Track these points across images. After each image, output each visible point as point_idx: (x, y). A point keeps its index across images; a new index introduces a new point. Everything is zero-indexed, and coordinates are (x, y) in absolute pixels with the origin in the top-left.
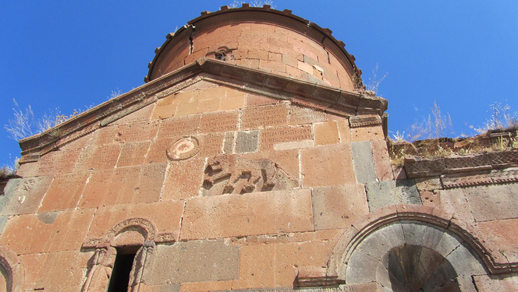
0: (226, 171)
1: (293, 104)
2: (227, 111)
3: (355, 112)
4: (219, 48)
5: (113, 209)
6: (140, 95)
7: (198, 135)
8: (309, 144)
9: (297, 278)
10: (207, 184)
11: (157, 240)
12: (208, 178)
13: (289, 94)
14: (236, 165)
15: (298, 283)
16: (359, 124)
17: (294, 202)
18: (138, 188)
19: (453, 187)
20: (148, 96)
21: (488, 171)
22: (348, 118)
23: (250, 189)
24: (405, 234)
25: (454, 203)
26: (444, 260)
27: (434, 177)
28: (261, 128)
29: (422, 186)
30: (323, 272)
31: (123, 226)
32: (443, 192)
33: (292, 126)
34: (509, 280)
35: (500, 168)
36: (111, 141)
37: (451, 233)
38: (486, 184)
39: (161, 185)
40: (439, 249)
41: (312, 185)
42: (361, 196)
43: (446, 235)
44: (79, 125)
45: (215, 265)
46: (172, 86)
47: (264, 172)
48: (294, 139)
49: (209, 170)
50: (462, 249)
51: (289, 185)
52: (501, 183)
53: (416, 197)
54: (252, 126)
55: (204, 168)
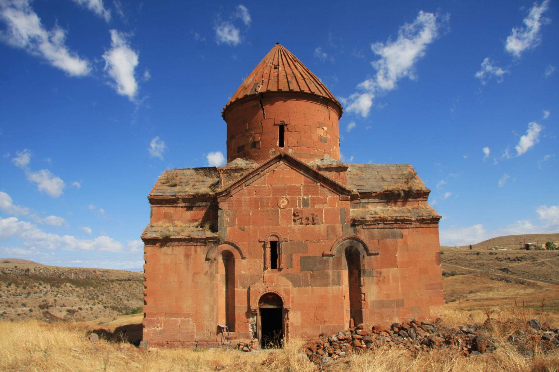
0: (301, 216)
1: (321, 185)
2: (296, 185)
3: (342, 194)
4: (280, 122)
5: (265, 227)
6: (258, 170)
7: (288, 197)
8: (327, 206)
9: (323, 253)
10: (295, 221)
11: (283, 240)
12: (295, 218)
13: (320, 181)
14: (304, 214)
15: (323, 255)
16: (343, 199)
17: (322, 229)
18: (271, 219)
19: (365, 229)
20: (262, 171)
21: (375, 224)
22: (340, 196)
23: (309, 224)
24: (351, 243)
25: (364, 234)
26: (358, 250)
27: (361, 225)
28: (310, 196)
29: (357, 227)
30: (330, 253)
31: (271, 235)
32: (363, 230)
33: (321, 197)
34: (371, 256)
35: (379, 224)
36: (253, 195)
37: (361, 243)
38: (374, 229)
39: (279, 219)
40: (358, 248)
41: (327, 224)
42: (340, 229)
43: (360, 244)
44: (237, 185)
45: (301, 249)
46: (271, 166)
47: (313, 218)
48: (322, 203)
49: (294, 214)
50: (363, 248)
51: (321, 223)
52: (378, 228)
53: (355, 231)
54: (307, 195)
55: (292, 213)
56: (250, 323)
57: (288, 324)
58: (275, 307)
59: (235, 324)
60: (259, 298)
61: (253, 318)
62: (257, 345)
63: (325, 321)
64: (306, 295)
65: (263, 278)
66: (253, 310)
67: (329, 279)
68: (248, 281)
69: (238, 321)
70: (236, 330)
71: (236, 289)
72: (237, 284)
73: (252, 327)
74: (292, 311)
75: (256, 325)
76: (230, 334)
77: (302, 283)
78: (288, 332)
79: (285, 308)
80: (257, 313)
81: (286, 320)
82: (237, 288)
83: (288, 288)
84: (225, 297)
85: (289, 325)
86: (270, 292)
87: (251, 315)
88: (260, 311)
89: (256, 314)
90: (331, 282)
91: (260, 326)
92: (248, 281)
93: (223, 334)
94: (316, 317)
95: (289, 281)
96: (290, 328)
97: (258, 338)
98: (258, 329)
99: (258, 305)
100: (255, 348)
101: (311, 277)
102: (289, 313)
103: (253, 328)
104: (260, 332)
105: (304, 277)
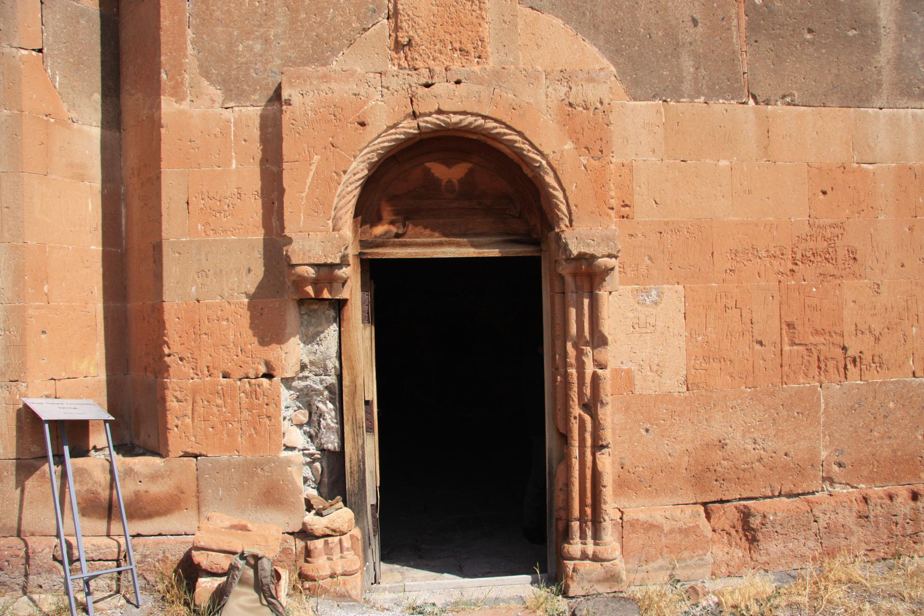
56: (287, 382)
57: (595, 377)
58: (494, 252)
59: (164, 387)
60: (359, 169)
61: (309, 339)
62: (352, 560)
63: (851, 352)
64: (723, 163)
65: (393, 15)
66: (311, 272)
67: (876, 49)
68: (267, 41)
69: (186, 368)
70: (176, 441)
71: (168, 106)
72: (179, 68)
73: (303, 416)
74: (622, 283)
75: (337, 394)
76: (129, 472)
77: (688, 64)
78: (598, 446)
79: (575, 249)
80: (345, 294)
81: (580, 354)
82: (179, 96)
83: (592, 93)
84: (98, 185)
85: (607, 388)
86: (455, 119)
87: (292, 315)
88: (364, 288)
89: (340, 305)
90: (887, 76)
91: (367, 403)
92: (267, 41)
93: (64, 475)
94: (790, 325)
95: (592, 49)
96: (607, 415)
97: (355, 504)
98: (355, 435)
99: (347, 230)
100: (325, 583)
101: (753, 27)
102: (603, 293)
103: (314, 417)
104: (371, 445)
105: (700, 29)
